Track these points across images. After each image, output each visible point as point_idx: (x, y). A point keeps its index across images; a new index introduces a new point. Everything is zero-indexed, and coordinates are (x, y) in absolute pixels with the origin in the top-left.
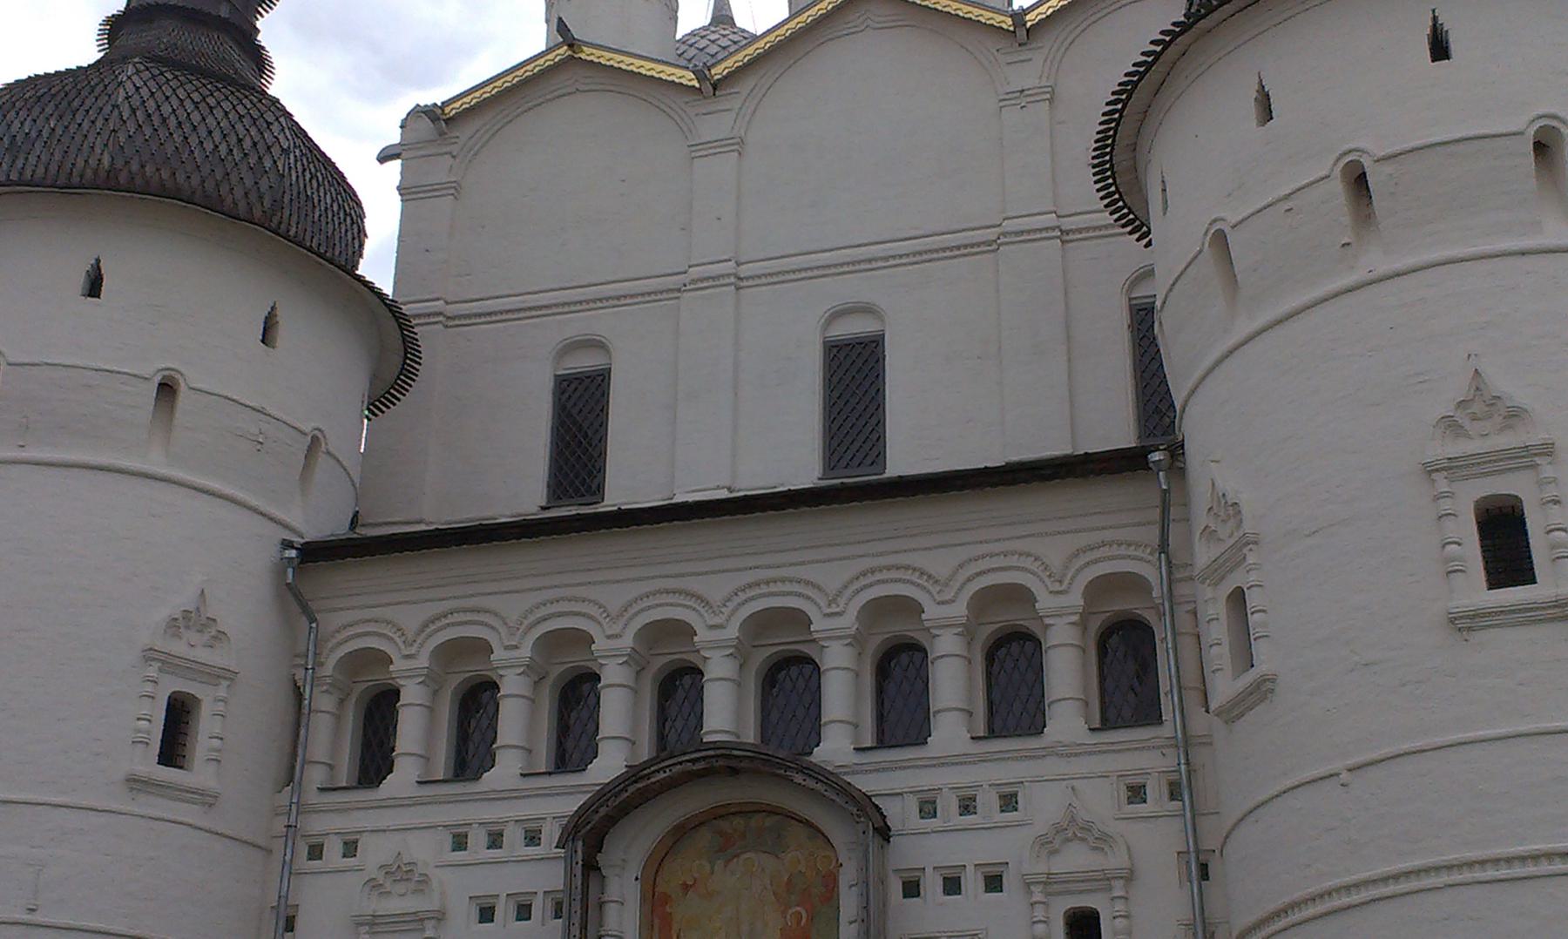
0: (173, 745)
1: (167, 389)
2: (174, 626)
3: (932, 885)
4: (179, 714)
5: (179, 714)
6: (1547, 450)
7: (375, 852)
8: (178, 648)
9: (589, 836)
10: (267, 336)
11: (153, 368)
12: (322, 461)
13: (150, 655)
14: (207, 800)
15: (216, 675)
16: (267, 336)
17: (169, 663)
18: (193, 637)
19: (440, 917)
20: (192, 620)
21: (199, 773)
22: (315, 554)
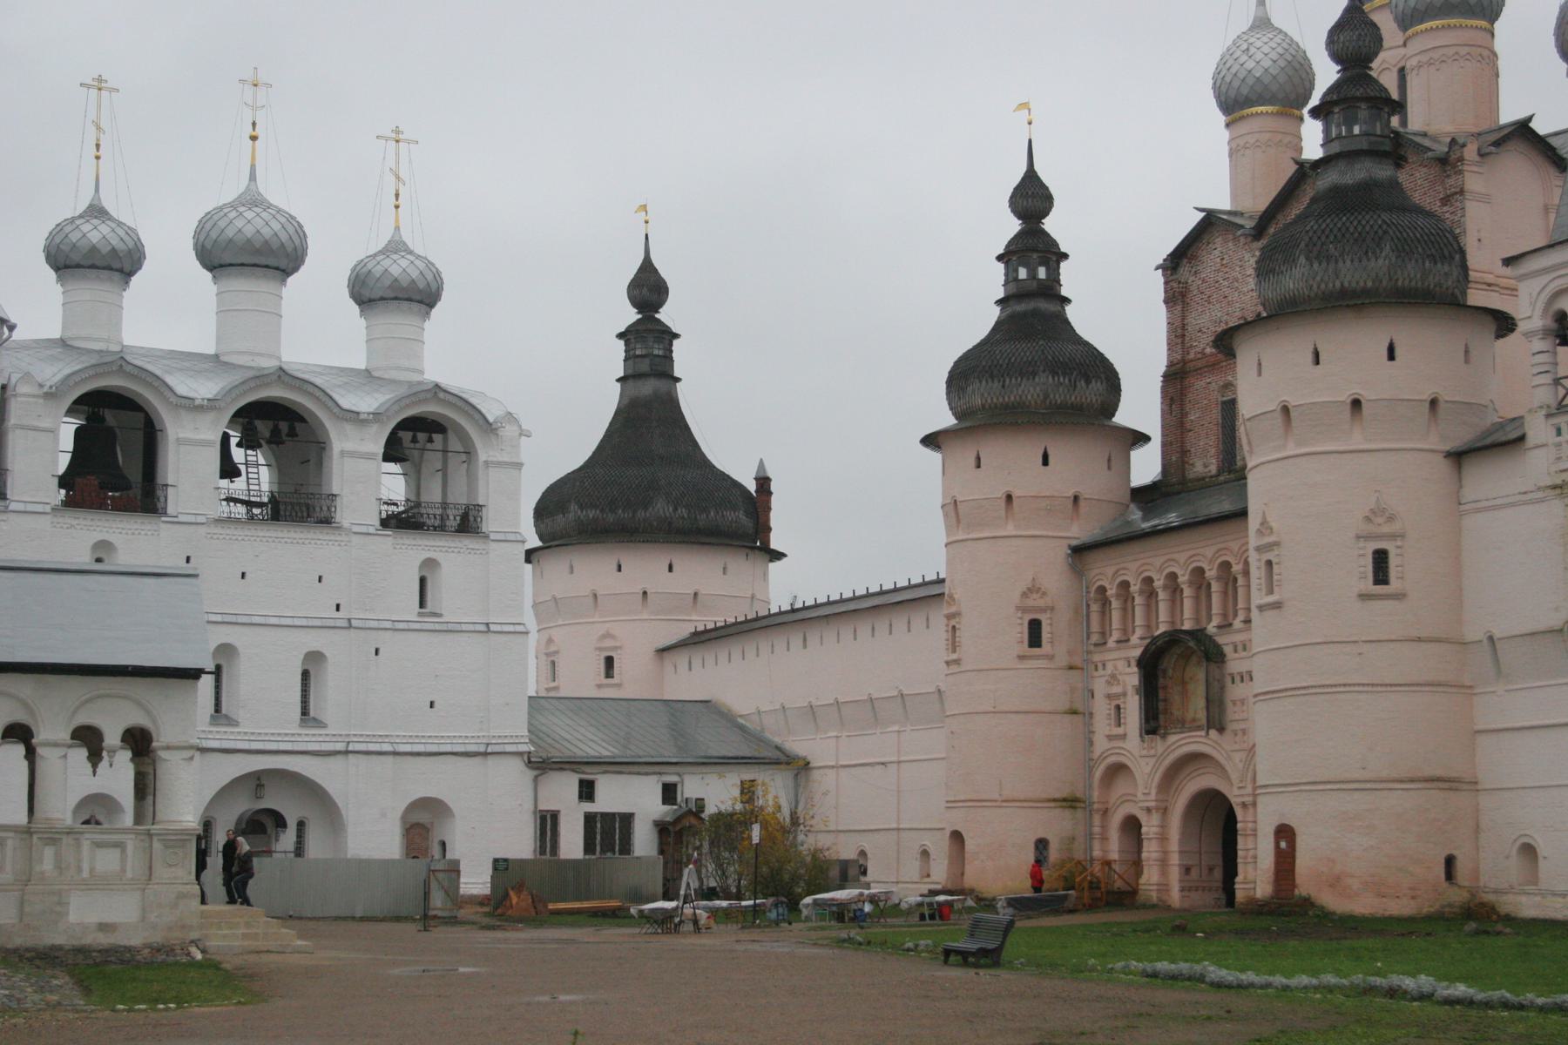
0: (1035, 638)
1: (1009, 498)
2: (1024, 595)
3: (1237, 679)
4: (1035, 628)
5: (1035, 628)
6: (1277, 544)
7: (1110, 666)
8: (1030, 603)
9: (1152, 665)
10: (1045, 462)
11: (1000, 493)
12: (1082, 503)
13: (1018, 608)
14: (1051, 658)
15: (1043, 610)
16: (1045, 462)
17: (1024, 610)
18: (1035, 596)
19: (1125, 694)
20: (1033, 590)
21: (1046, 647)
22: (1080, 551)
